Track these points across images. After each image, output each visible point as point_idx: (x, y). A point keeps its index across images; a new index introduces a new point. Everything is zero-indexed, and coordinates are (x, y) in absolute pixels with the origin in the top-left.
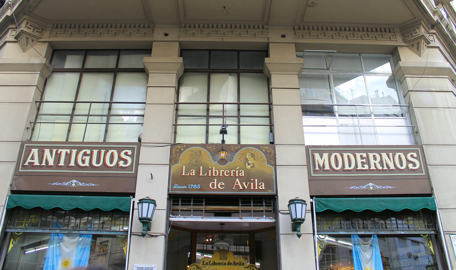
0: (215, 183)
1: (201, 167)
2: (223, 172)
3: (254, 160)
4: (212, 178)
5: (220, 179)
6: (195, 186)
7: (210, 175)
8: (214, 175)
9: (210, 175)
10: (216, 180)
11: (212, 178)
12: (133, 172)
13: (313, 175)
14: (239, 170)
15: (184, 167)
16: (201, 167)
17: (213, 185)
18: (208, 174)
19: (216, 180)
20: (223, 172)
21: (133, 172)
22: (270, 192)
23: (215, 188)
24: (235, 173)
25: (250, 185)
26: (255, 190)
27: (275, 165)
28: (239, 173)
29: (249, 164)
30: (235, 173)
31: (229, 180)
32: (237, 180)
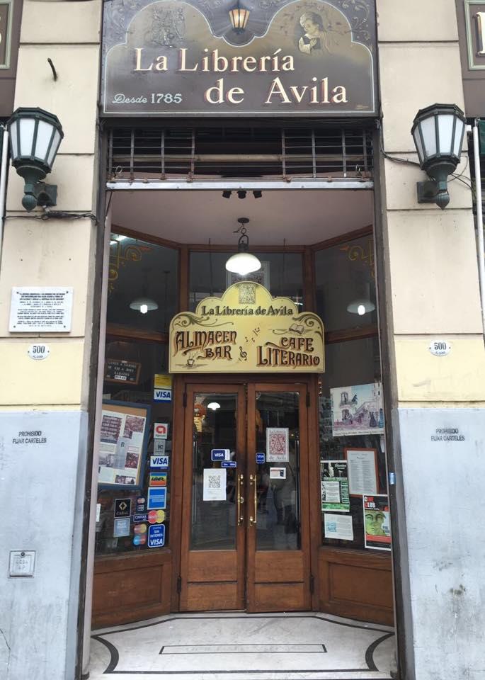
0: (221, 90)
1: (184, 51)
2: (240, 63)
3: (321, 29)
4: (212, 77)
5: (232, 78)
6: (168, 98)
7: (206, 69)
8: (216, 69)
9: (206, 69)
10: (221, 81)
11: (212, 77)
12: (7, 65)
13: (472, 66)
14: (280, 56)
15: (139, 50)
16: (184, 51)
17: (215, 95)
18: (201, 66)
19: (221, 81)
20: (240, 63)
21: (7, 65)
22: (360, 111)
23: (221, 100)
24: (270, 64)
25: (309, 93)
26: (320, 105)
27: (375, 43)
28: (281, 63)
29: (307, 41)
30: (270, 64)
31: (258, 82)
32: (277, 81)
